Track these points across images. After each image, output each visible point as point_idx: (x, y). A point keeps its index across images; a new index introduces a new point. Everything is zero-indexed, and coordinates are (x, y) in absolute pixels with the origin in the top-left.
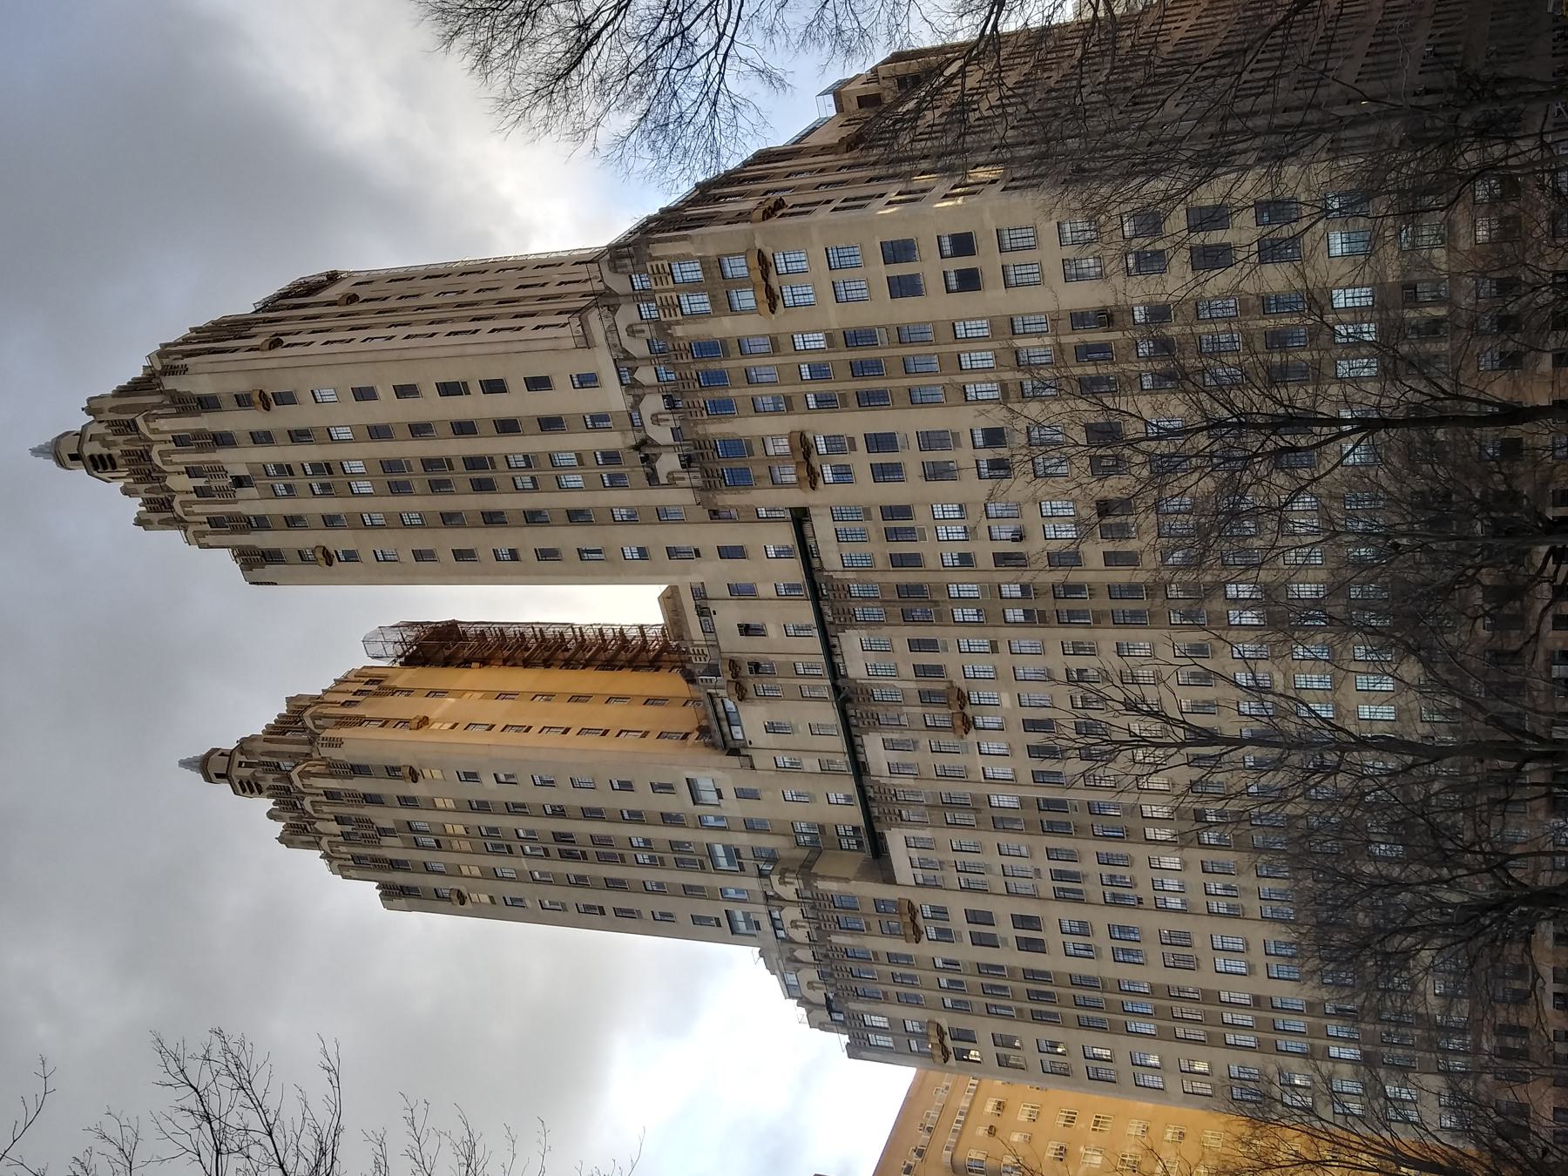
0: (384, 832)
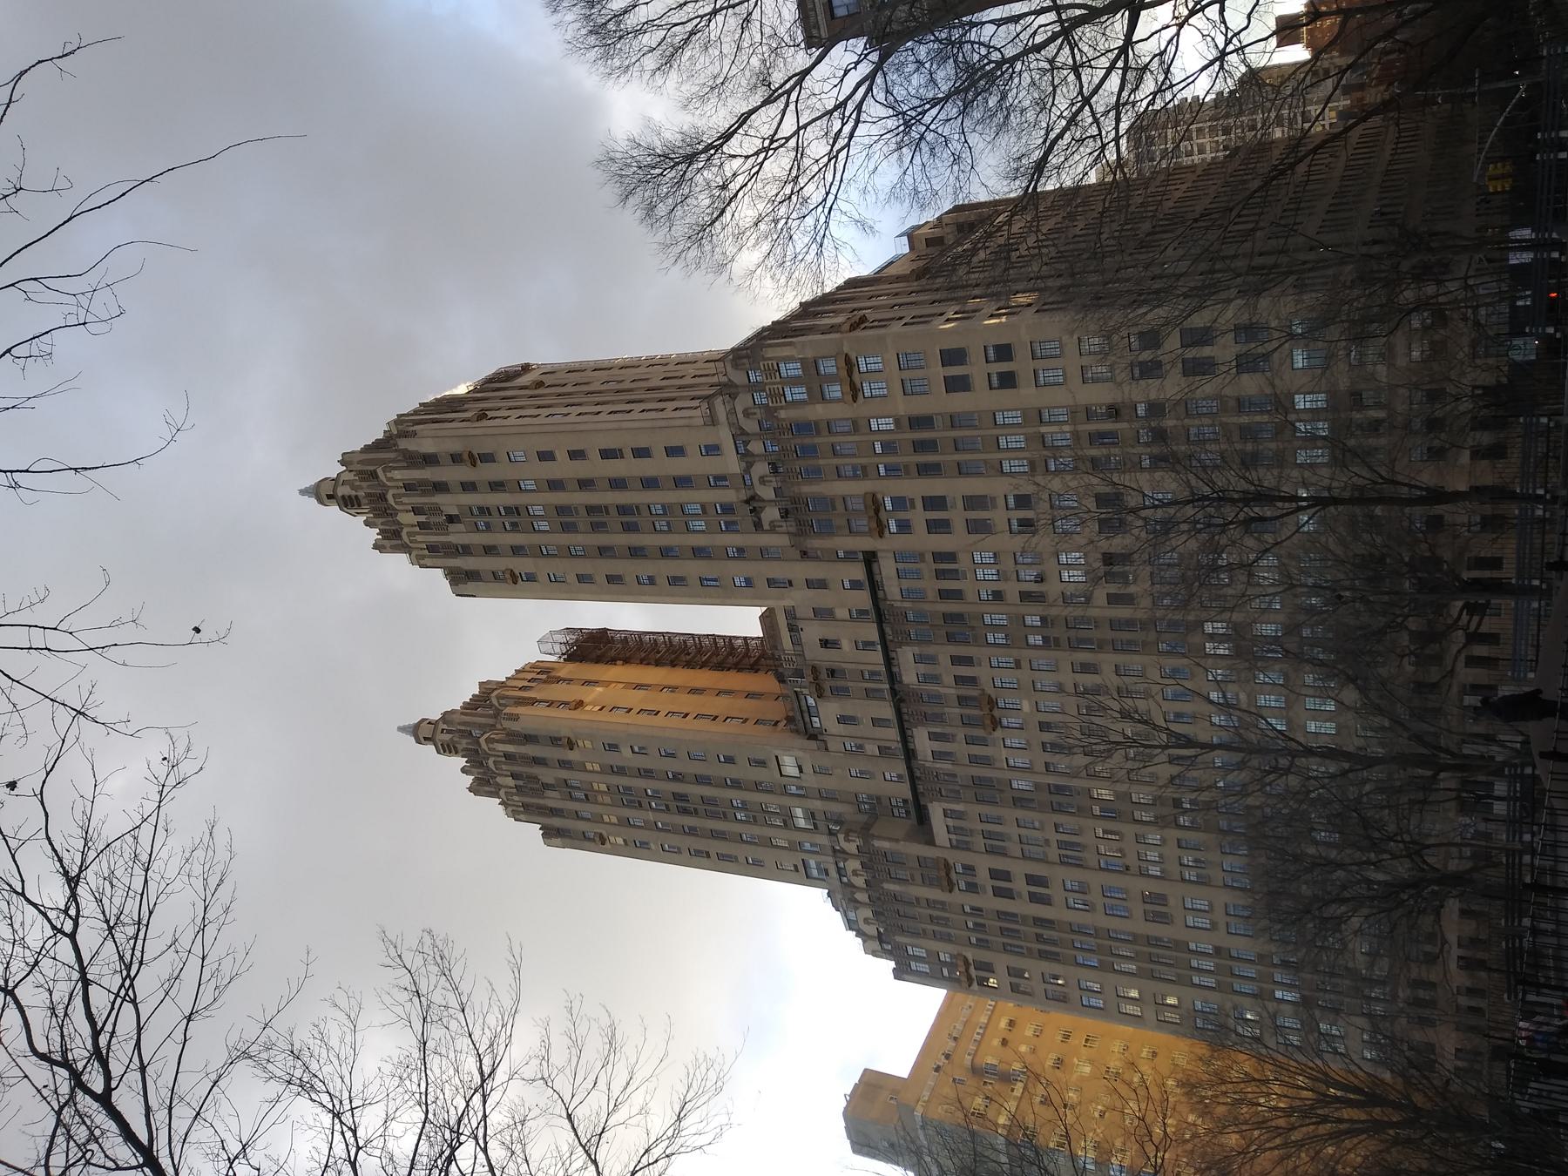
0: (546, 786)
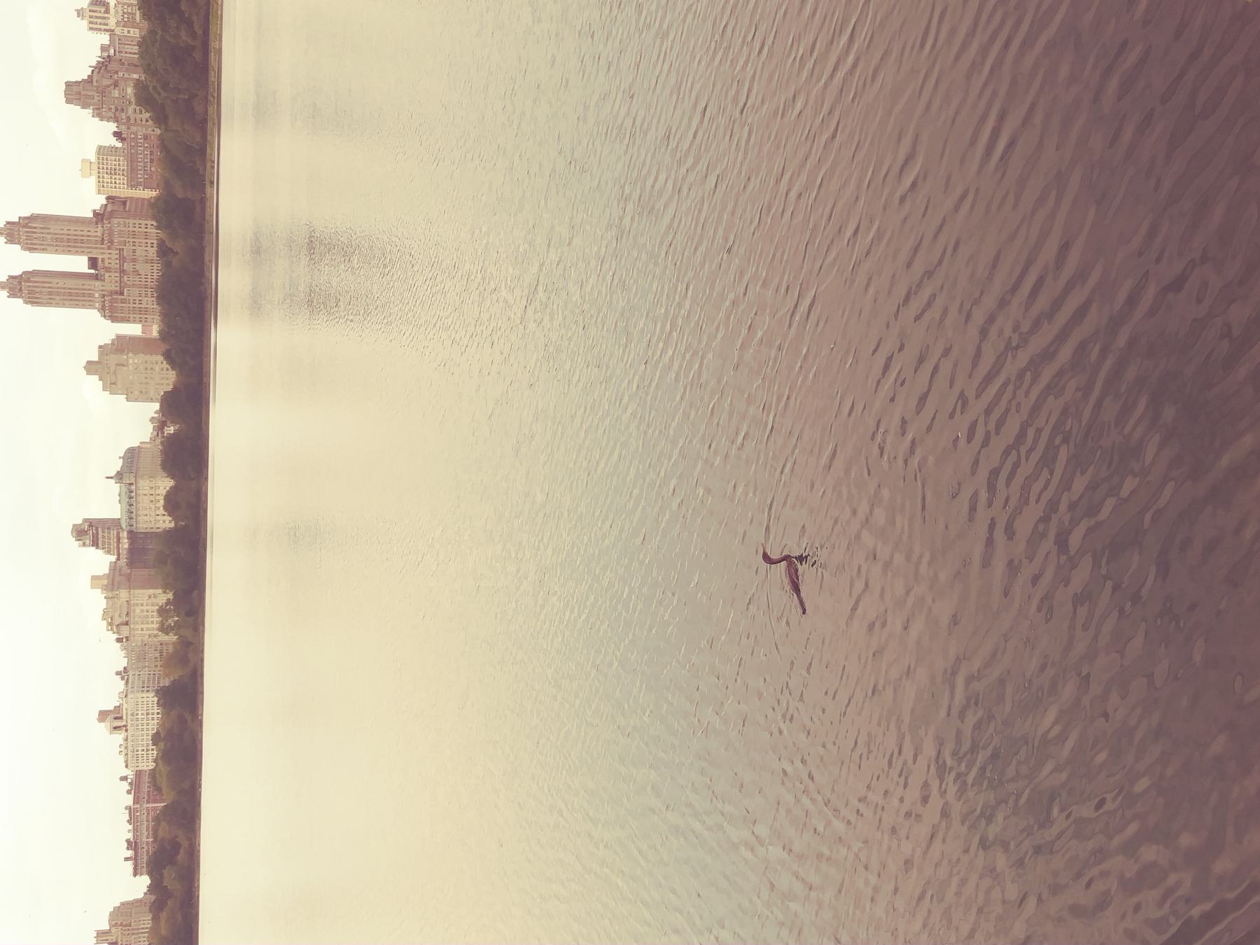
0: (37, 292)
